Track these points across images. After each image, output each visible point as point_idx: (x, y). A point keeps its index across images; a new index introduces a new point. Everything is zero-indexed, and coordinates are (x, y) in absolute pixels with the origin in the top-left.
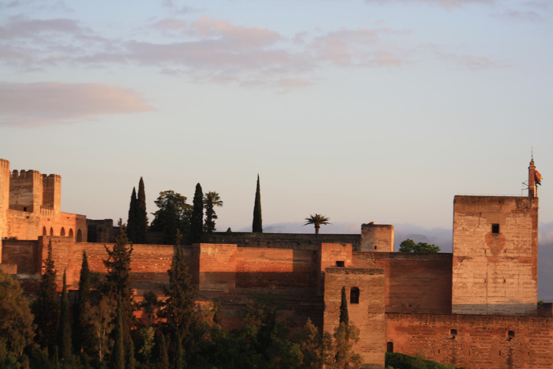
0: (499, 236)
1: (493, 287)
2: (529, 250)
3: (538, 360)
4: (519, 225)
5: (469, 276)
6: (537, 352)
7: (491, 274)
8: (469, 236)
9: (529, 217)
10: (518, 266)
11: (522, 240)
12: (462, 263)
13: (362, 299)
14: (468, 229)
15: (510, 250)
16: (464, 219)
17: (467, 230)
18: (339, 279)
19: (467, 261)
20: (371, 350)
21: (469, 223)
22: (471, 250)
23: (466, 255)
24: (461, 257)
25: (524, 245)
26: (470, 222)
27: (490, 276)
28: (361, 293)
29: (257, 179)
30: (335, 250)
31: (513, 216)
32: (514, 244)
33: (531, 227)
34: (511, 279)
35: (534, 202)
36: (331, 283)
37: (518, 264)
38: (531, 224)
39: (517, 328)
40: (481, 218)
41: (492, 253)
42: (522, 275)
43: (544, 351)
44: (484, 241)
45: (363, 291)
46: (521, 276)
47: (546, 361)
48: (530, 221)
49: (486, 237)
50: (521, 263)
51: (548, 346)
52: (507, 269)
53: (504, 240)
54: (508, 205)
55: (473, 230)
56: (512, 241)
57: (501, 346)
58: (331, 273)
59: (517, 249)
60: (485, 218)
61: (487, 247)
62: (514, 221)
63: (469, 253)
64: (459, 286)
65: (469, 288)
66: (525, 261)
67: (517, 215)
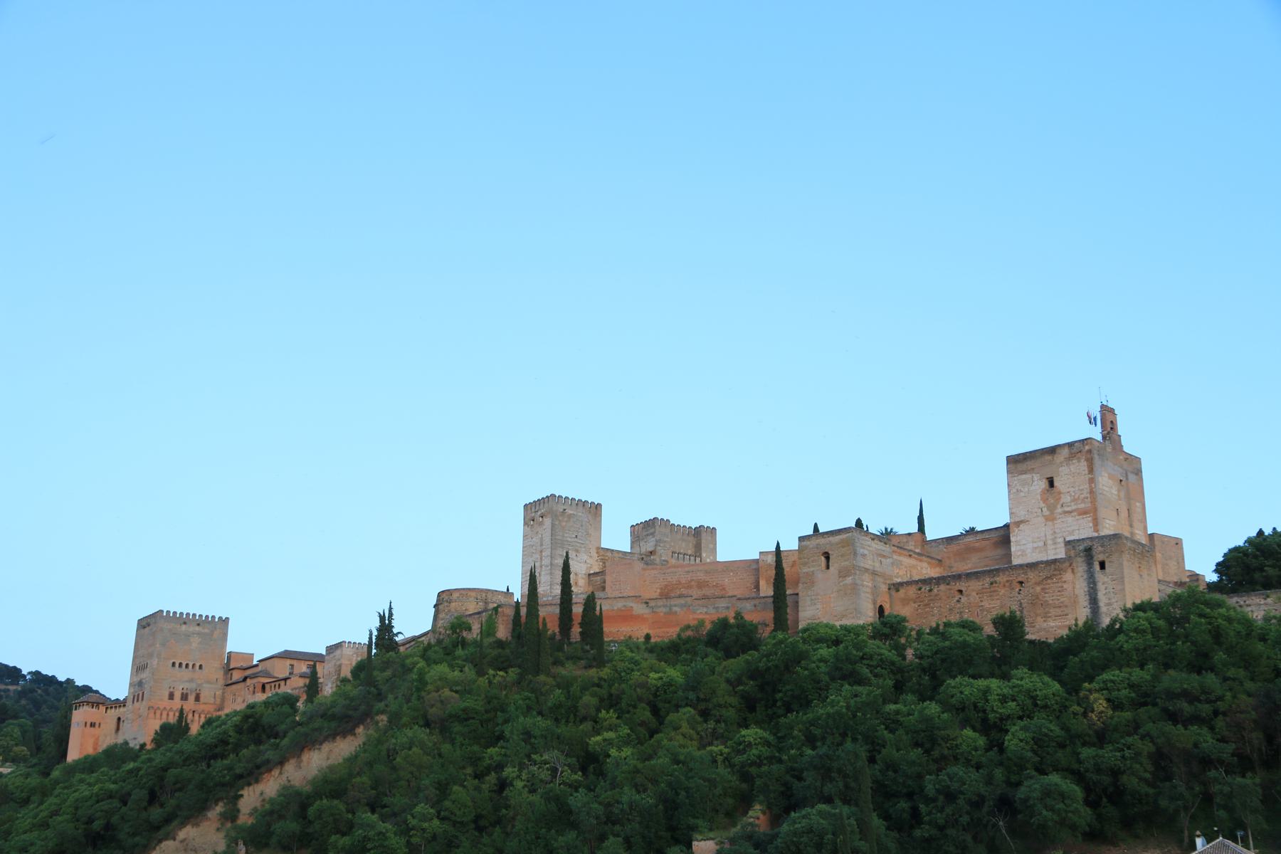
3: (1053, 612)
6: (1051, 602)
11: (1079, 489)
12: (1020, 528)
14: (1022, 489)
17: (1021, 491)
18: (811, 546)
24: (1018, 522)
27: (1049, 537)
32: (1071, 496)
33: (1087, 472)
35: (1087, 444)
37: (1077, 517)
39: (1026, 577)
40: (1034, 475)
44: (1040, 498)
53: (1060, 493)
55: (1027, 490)
58: (804, 541)
59: (1074, 500)
61: (1043, 505)
65: (1029, 555)
66: (1083, 513)
67: (1070, 462)
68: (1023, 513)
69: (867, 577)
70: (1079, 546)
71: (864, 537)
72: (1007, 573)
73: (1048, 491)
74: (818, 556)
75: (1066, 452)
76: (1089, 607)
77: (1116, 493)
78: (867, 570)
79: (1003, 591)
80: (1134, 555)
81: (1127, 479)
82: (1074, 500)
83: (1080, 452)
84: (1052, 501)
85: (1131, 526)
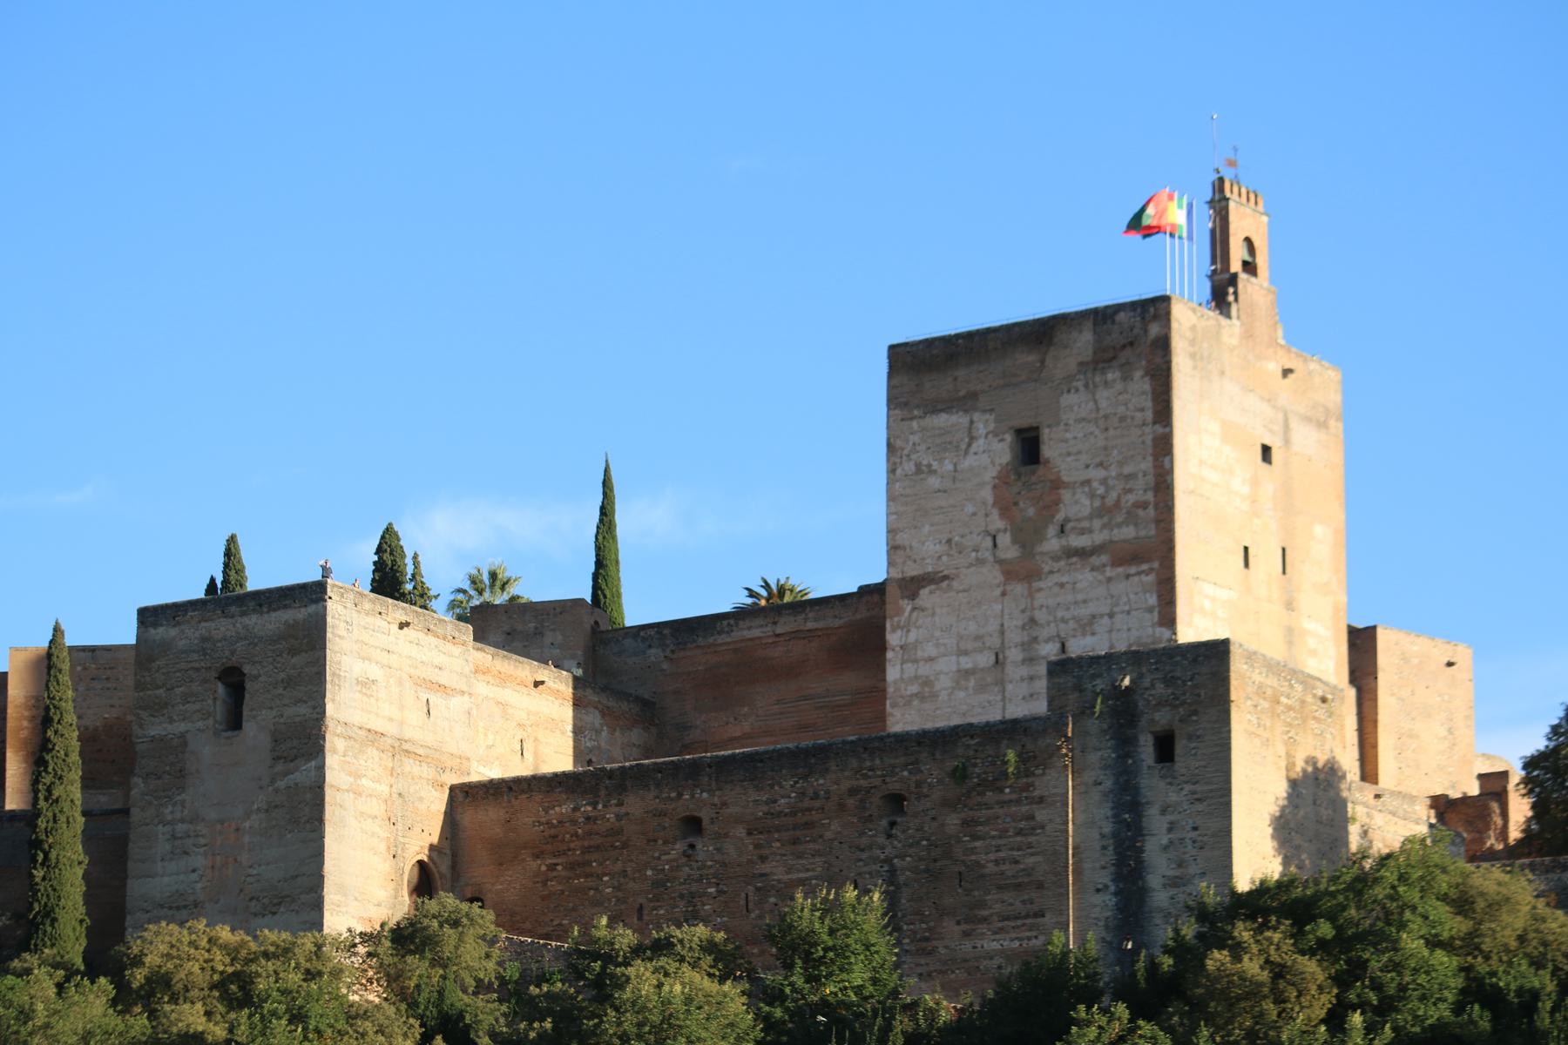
0: (1041, 470)
1: (1022, 679)
2: (1145, 508)
4: (1106, 417)
5: (942, 649)
6: (991, 868)
7: (1016, 627)
8: (939, 491)
9: (1142, 377)
10: (1110, 580)
11: (1119, 476)
12: (918, 602)
13: (252, 710)
14: (935, 465)
15: (1078, 520)
16: (923, 429)
17: (932, 472)
18: (182, 644)
19: (931, 592)
20: (280, 904)
21: (938, 441)
22: (945, 548)
23: (930, 569)
24: (912, 578)
25: (1125, 494)
26: (941, 435)
27: (1015, 637)
28: (248, 685)
29: (598, 499)
30: (520, 628)
31: (1086, 386)
32: (1092, 496)
33: (1149, 415)
34: (1084, 635)
35: (1156, 317)
36: (155, 665)
37: (1109, 572)
38: (1149, 404)
40: (976, 416)
41: (1017, 546)
42: (1123, 612)
43: (1017, 862)
44: (990, 500)
45: (256, 677)
46: (1118, 618)
47: (1023, 902)
48: (1144, 393)
49: (995, 487)
50: (1120, 565)
51: (1031, 839)
52: (1070, 598)
53: (1057, 484)
54: (1066, 347)
56: (1088, 482)
57: (861, 860)
58: (155, 625)
60: (992, 410)
62: (1091, 405)
63: (940, 557)
64: (909, 693)
65: (943, 696)
66: (1129, 556)
68: (931, 548)
69: (373, 761)
70: (1094, 677)
71: (370, 619)
72: (854, 763)
73: (1019, 475)
74: (205, 681)
75: (1084, 340)
76: (1112, 888)
77: (1245, 490)
78: (374, 736)
79: (835, 826)
80: (1274, 715)
81: (1287, 441)
82: (1104, 511)
83: (1131, 344)
84: (1031, 512)
85: (1290, 605)
